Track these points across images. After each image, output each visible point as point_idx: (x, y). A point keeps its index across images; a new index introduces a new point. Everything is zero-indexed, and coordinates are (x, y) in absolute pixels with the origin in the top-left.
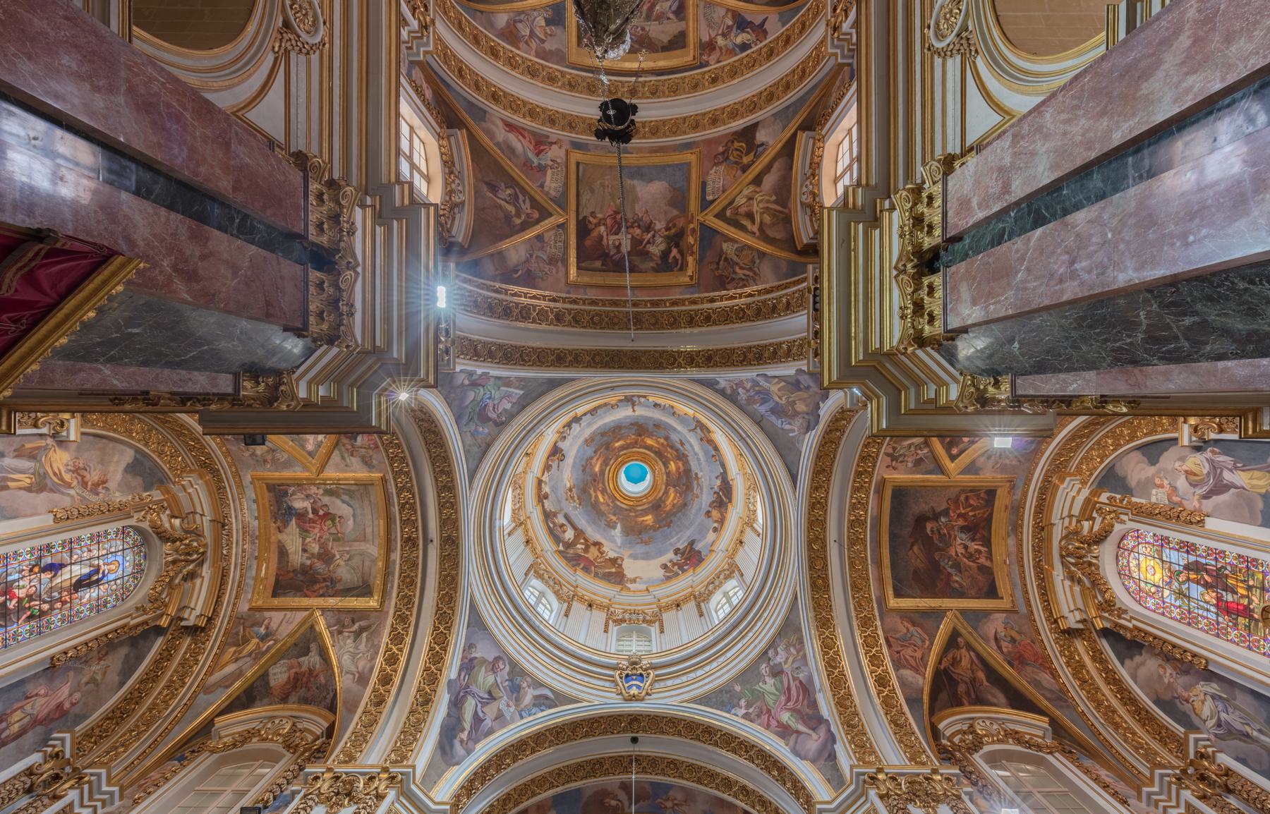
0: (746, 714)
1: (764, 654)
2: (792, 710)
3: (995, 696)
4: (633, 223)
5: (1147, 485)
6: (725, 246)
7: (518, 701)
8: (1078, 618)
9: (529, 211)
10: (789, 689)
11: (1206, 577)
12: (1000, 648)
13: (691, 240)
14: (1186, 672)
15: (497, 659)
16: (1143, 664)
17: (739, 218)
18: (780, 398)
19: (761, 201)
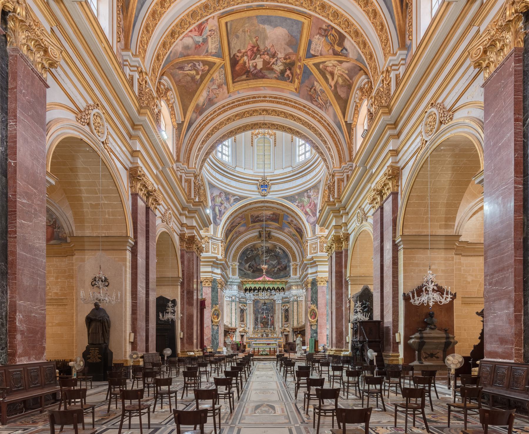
4: (264, 52)
6: (316, 83)
9: (203, 68)
13: (298, 71)
17: (327, 72)
19: (340, 70)
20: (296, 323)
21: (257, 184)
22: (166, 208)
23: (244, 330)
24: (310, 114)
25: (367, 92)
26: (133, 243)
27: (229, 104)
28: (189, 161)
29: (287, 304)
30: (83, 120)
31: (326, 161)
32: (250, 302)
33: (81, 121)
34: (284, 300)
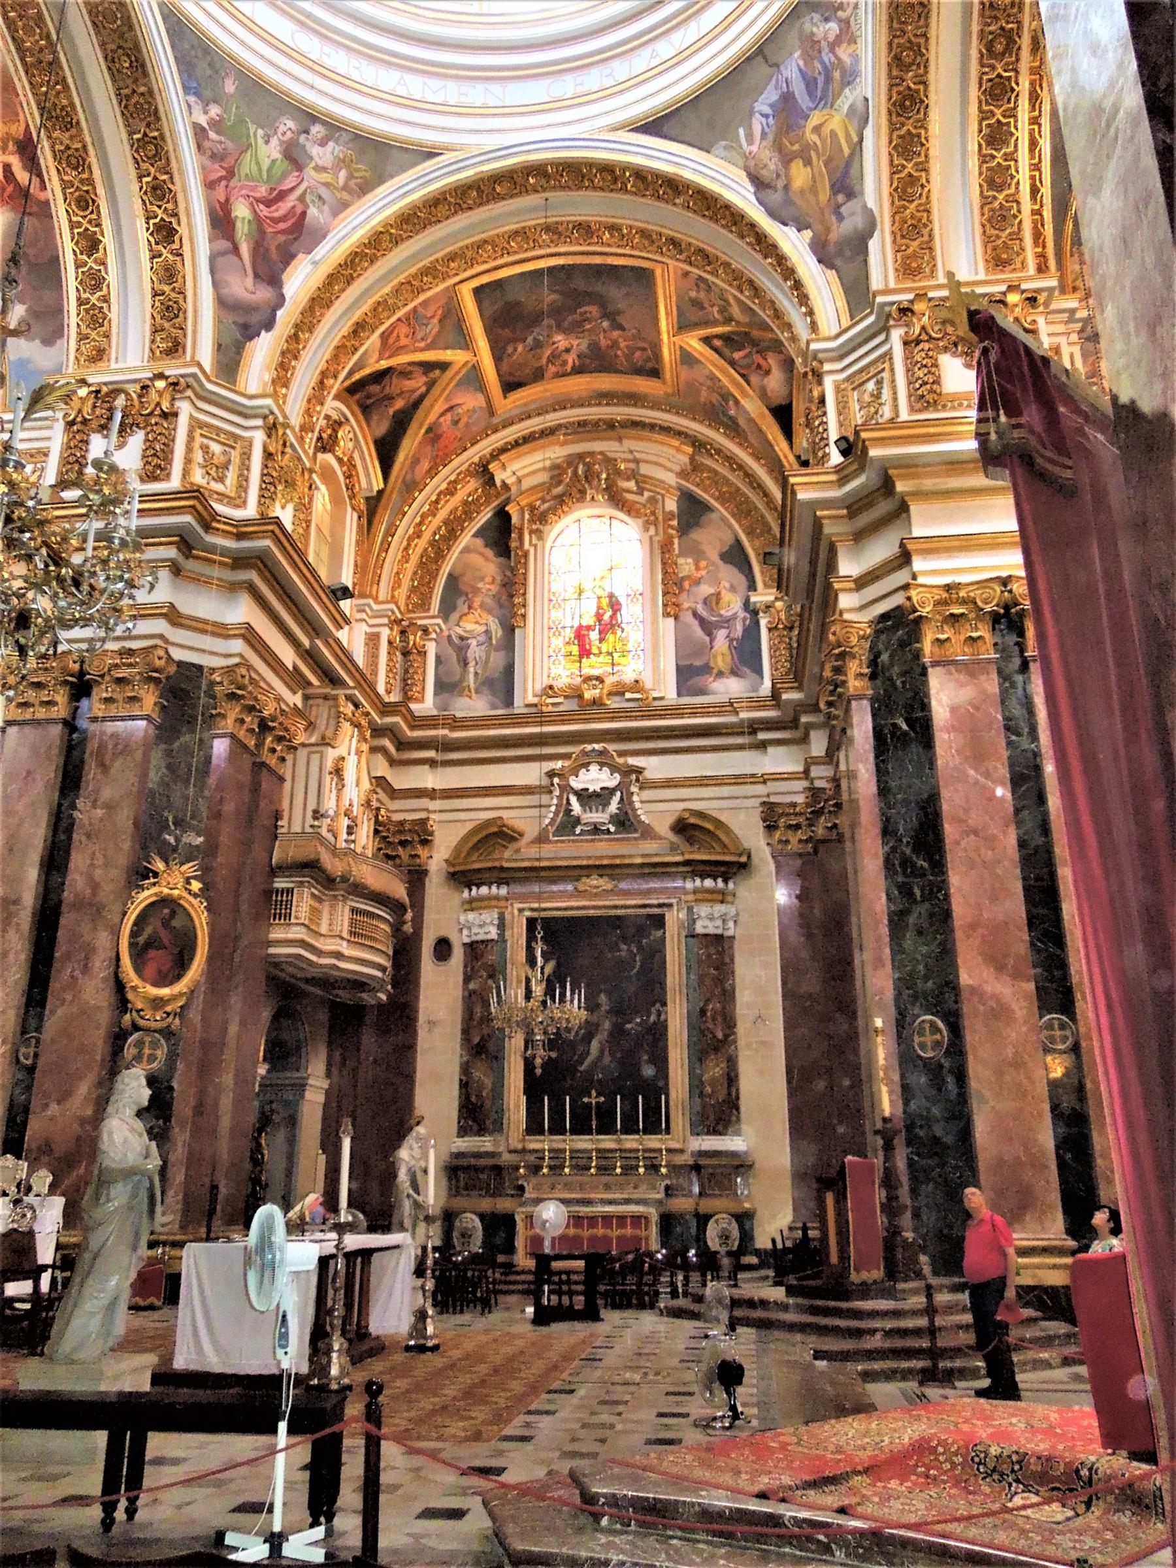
0: (203, 129)
1: (309, 117)
2: (258, 221)
3: (379, 421)
5: (697, 554)
8: (508, 482)
10: (282, 195)
11: (606, 617)
12: (442, 414)
14: (501, 606)
16: (487, 559)
18: (817, 129)
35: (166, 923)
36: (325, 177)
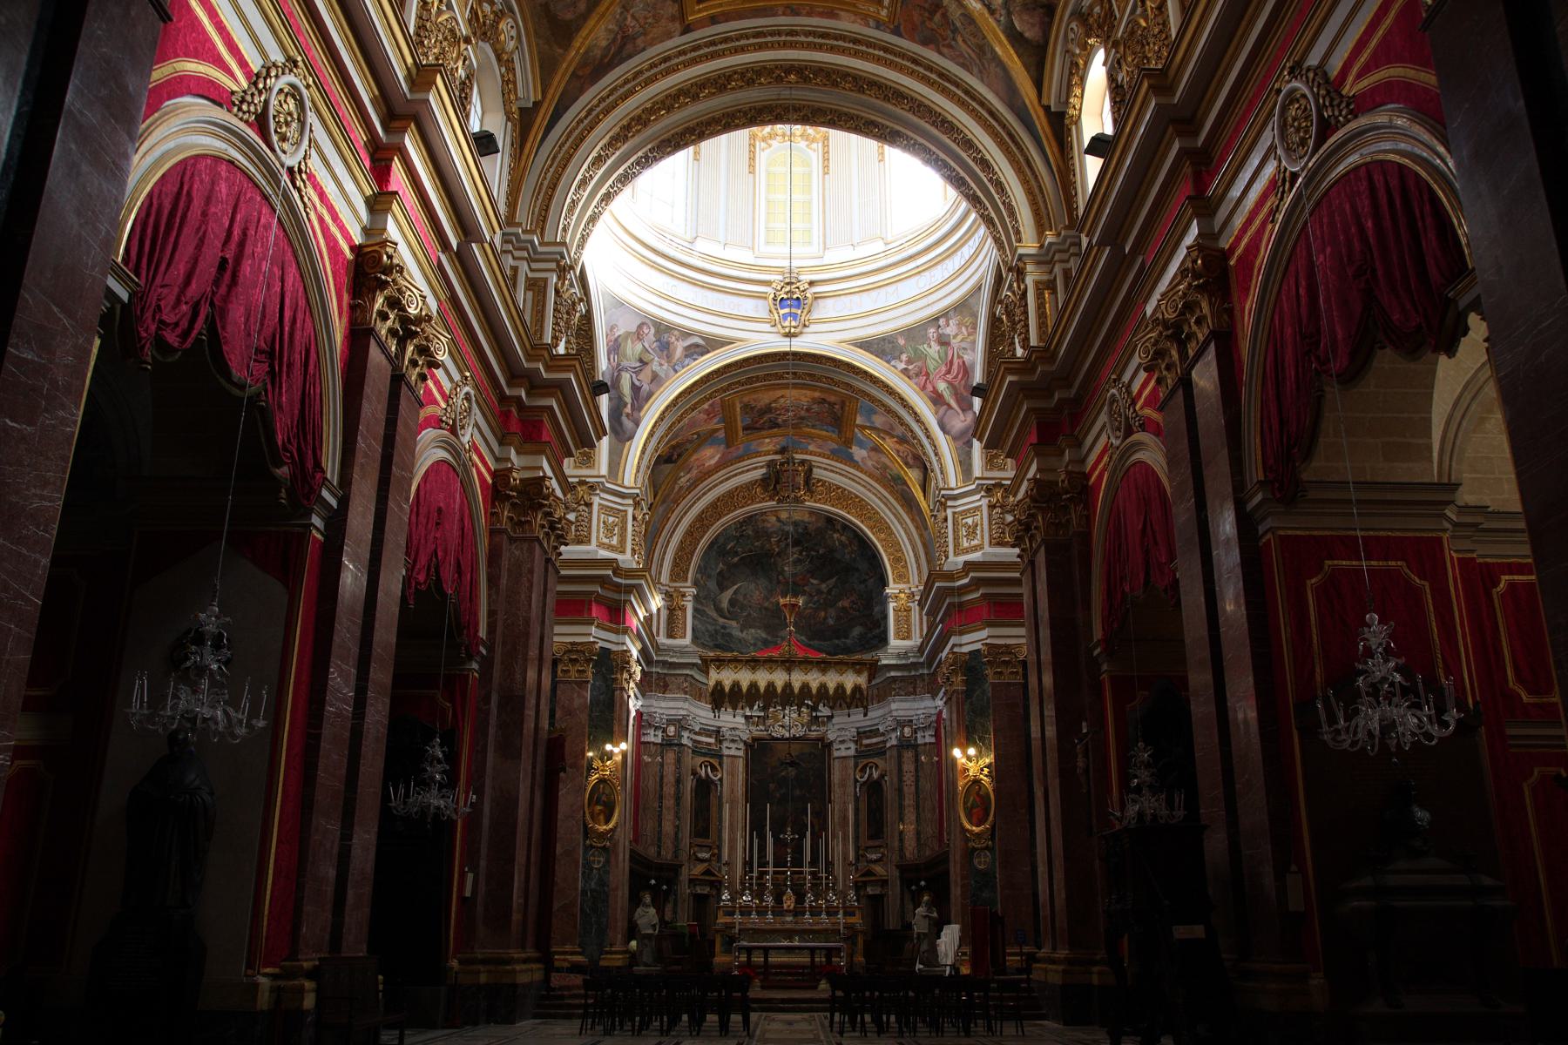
0: (906, 369)
1: (934, 320)
7: (668, 357)
10: (951, 362)
15: (640, 327)
20: (914, 844)
21: (761, 297)
22: (457, 377)
23: (708, 872)
24: (935, 82)
25: (1100, 27)
26: (334, 502)
27: (683, 53)
28: (544, 221)
29: (876, 760)
30: (245, 107)
31: (994, 225)
32: (733, 752)
33: (240, 109)
34: (866, 742)
35: (978, 794)
36: (960, 338)
